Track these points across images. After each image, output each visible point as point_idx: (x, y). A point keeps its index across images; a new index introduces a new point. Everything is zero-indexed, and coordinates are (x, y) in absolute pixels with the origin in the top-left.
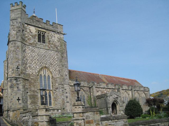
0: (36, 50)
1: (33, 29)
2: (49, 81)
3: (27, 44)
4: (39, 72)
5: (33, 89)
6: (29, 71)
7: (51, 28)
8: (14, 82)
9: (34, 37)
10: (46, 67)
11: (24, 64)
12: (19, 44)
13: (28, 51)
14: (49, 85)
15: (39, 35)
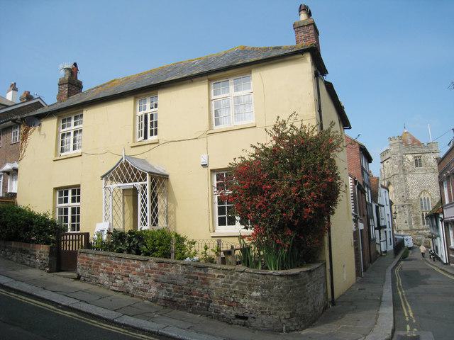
0: (415, 176)
1: (410, 157)
2: (429, 204)
3: (407, 173)
4: (419, 196)
5: (415, 211)
6: (411, 197)
7: (426, 150)
8: (402, 208)
9: (411, 164)
10: (425, 190)
11: (407, 191)
12: (402, 176)
13: (409, 179)
14: (429, 207)
15: (416, 160)
